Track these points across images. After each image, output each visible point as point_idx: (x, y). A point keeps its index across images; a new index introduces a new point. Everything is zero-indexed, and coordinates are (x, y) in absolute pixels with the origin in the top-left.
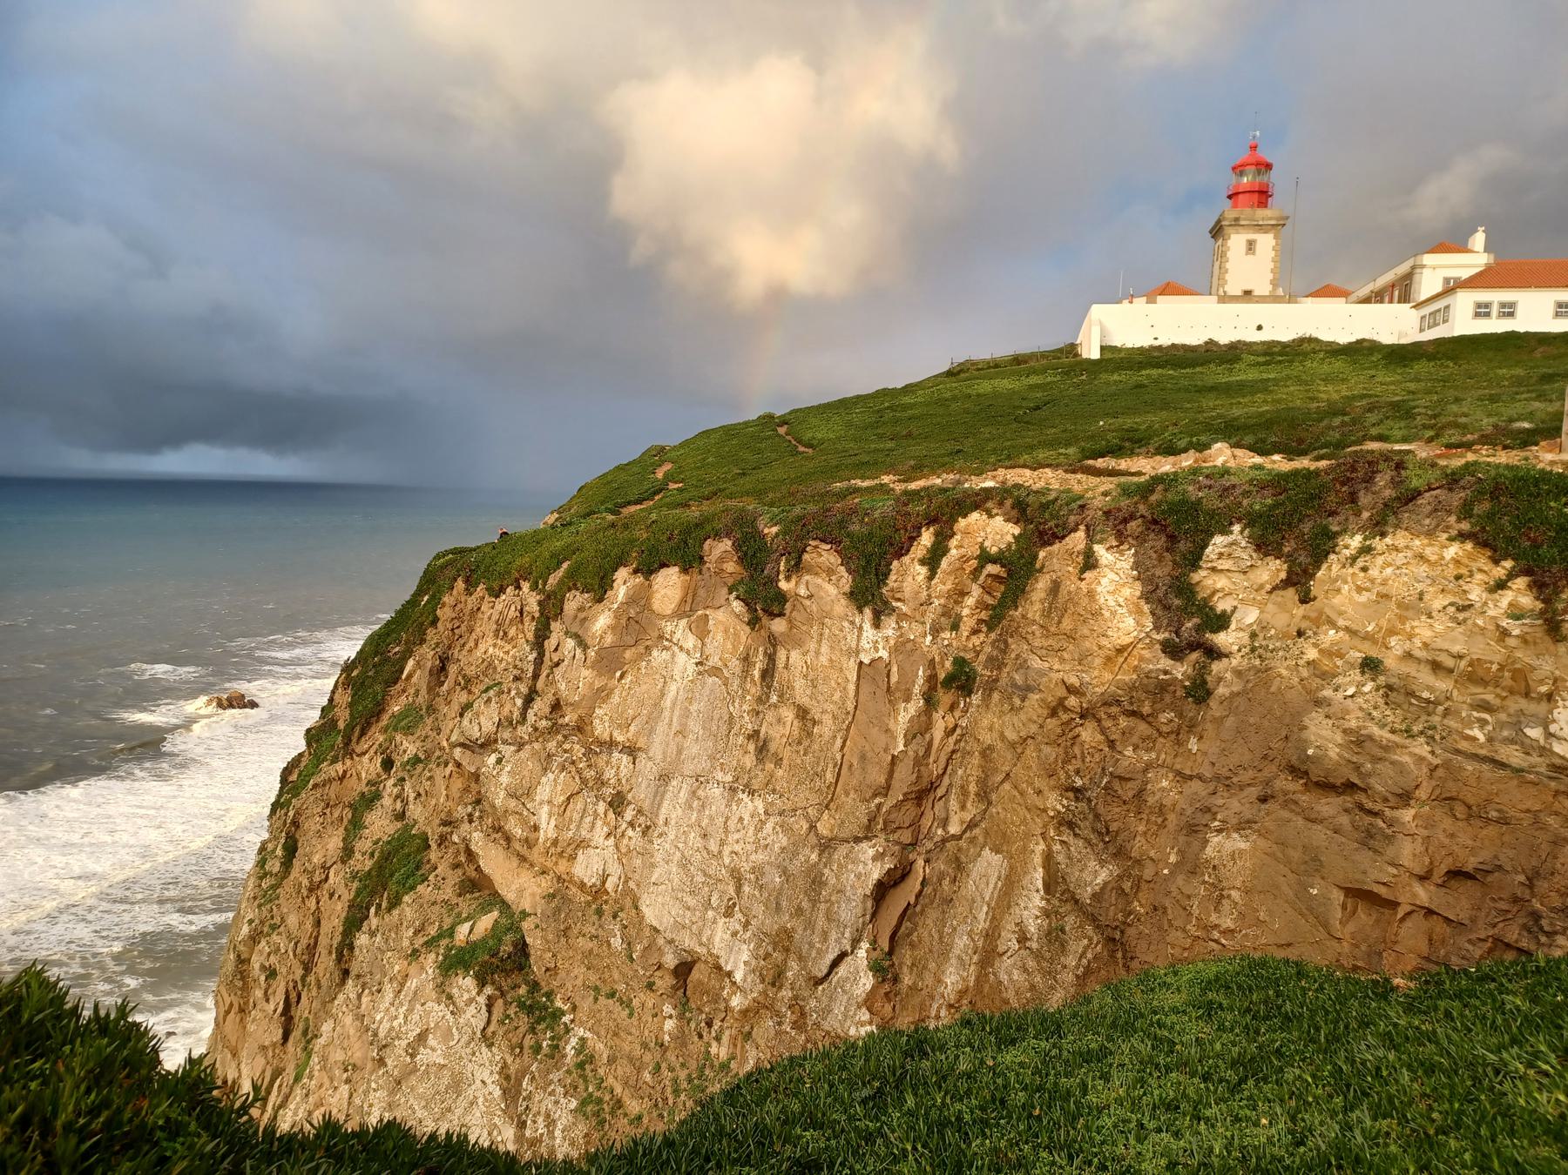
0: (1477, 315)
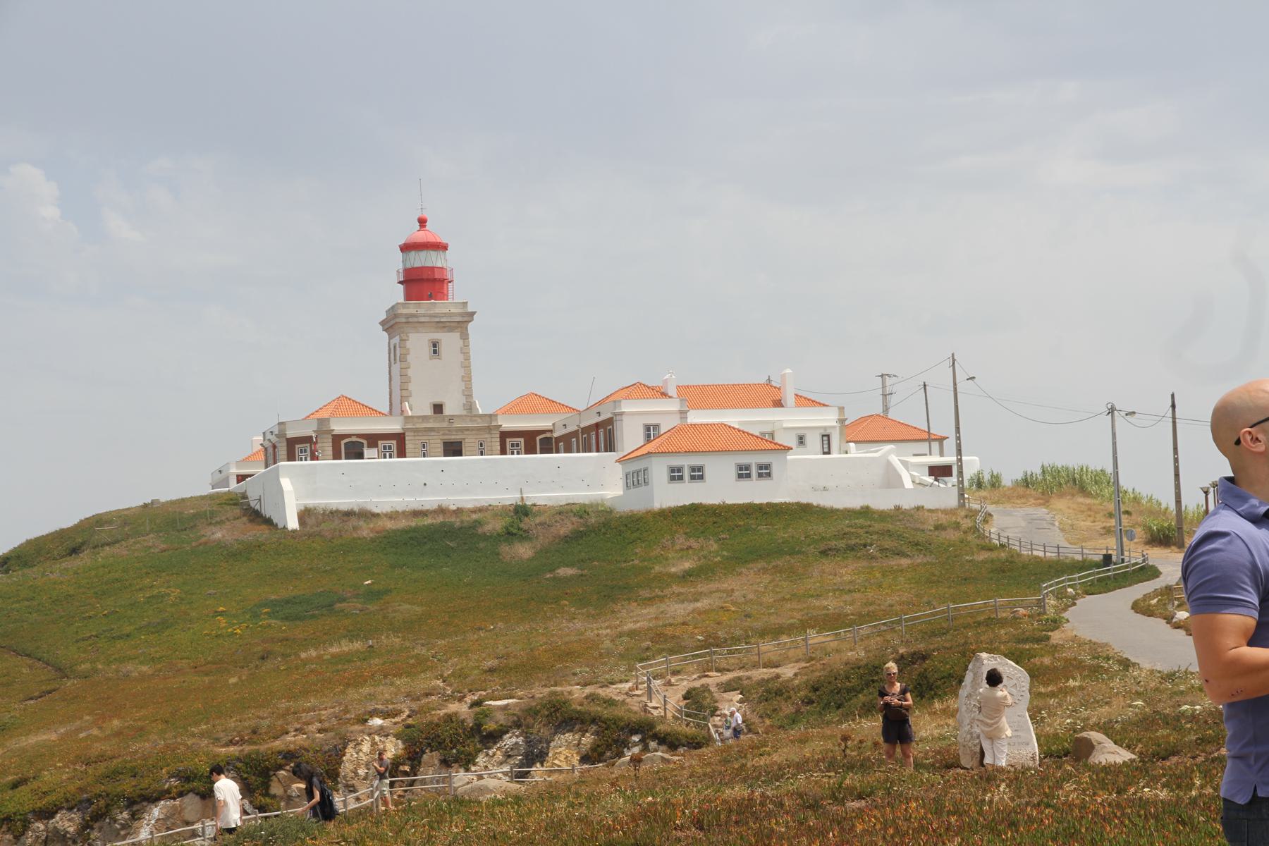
0: (672, 479)
